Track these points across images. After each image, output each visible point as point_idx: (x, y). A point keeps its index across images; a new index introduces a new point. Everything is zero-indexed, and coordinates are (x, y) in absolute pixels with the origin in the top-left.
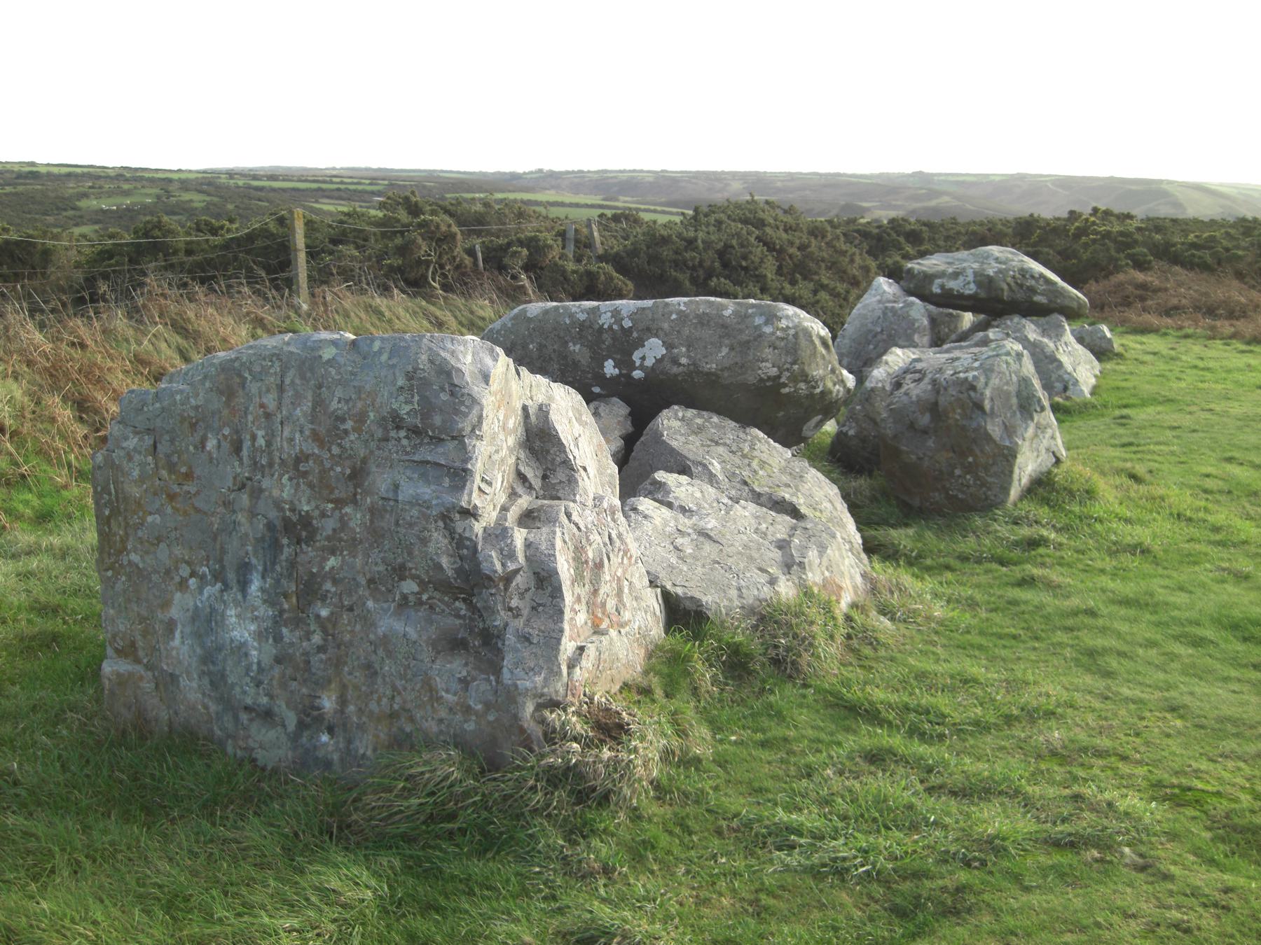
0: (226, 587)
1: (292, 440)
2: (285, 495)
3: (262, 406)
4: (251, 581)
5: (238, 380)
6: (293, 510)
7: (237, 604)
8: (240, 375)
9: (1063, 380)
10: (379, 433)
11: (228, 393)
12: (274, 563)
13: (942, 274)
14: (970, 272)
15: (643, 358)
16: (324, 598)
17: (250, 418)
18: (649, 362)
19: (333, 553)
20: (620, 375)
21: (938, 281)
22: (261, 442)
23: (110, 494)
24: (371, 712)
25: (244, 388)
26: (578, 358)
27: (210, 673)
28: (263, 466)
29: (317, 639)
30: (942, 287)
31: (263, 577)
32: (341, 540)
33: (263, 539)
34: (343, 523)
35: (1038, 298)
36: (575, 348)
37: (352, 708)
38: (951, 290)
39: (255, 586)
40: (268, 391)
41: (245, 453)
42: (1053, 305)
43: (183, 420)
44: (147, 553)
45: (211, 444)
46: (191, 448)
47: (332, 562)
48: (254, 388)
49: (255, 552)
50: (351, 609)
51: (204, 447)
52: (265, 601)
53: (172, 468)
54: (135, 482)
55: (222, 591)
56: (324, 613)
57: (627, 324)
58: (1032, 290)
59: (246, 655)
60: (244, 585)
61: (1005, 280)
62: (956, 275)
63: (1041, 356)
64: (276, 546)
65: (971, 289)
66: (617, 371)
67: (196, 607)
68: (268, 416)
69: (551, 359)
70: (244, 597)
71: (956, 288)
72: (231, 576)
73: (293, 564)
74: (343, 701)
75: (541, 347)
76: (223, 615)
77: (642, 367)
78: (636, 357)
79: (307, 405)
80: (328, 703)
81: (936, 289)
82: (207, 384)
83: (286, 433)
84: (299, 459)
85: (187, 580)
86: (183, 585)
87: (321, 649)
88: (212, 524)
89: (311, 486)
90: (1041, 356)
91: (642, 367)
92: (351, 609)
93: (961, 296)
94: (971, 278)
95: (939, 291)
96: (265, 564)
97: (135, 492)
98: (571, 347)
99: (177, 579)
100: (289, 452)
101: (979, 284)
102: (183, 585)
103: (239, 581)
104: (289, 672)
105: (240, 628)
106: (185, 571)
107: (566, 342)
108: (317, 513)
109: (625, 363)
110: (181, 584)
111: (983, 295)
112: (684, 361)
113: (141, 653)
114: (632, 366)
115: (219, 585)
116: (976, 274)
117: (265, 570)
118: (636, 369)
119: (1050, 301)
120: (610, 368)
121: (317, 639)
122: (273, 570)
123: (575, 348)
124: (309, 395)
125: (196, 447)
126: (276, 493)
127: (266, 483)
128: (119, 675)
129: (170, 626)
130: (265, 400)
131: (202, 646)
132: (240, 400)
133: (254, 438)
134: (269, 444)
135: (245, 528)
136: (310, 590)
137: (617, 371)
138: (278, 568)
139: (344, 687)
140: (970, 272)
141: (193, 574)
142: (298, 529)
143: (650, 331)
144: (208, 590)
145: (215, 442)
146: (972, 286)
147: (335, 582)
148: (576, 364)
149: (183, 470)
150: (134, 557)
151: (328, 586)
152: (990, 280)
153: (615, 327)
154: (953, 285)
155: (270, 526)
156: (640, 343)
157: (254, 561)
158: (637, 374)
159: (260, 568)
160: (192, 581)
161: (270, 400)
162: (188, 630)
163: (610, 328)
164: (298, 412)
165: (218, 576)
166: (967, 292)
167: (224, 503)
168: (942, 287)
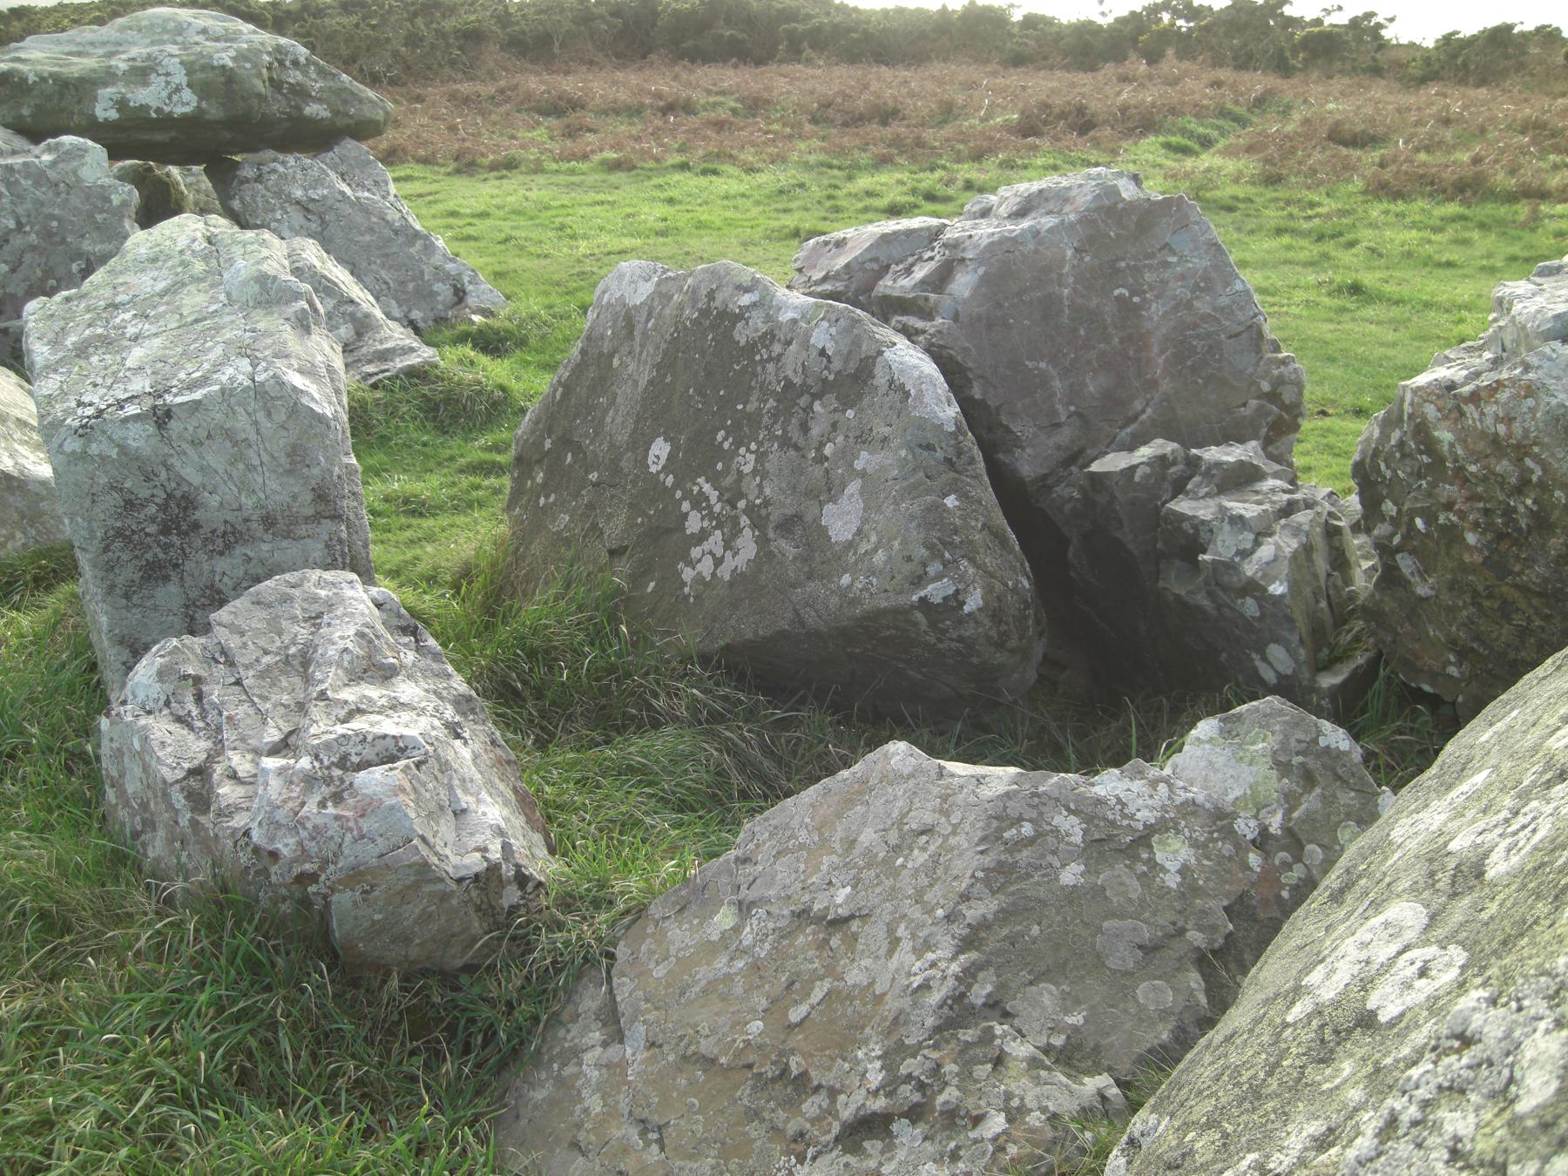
9: (448, 275)
13: (109, 77)
14: (173, 65)
21: (106, 93)
30: (122, 104)
35: (314, 110)
38: (144, 108)
42: (341, 122)
58: (300, 92)
61: (260, 75)
62: (142, 73)
63: (387, 232)
65: (186, 104)
71: (154, 104)
81: (104, 111)
90: (387, 232)
93: (165, 121)
94: (180, 77)
95: (113, 115)
111: (214, 112)
119: (336, 113)
140: (173, 65)
146: (187, 94)
152: (228, 76)
154: (148, 96)
166: (179, 110)
168: (122, 104)
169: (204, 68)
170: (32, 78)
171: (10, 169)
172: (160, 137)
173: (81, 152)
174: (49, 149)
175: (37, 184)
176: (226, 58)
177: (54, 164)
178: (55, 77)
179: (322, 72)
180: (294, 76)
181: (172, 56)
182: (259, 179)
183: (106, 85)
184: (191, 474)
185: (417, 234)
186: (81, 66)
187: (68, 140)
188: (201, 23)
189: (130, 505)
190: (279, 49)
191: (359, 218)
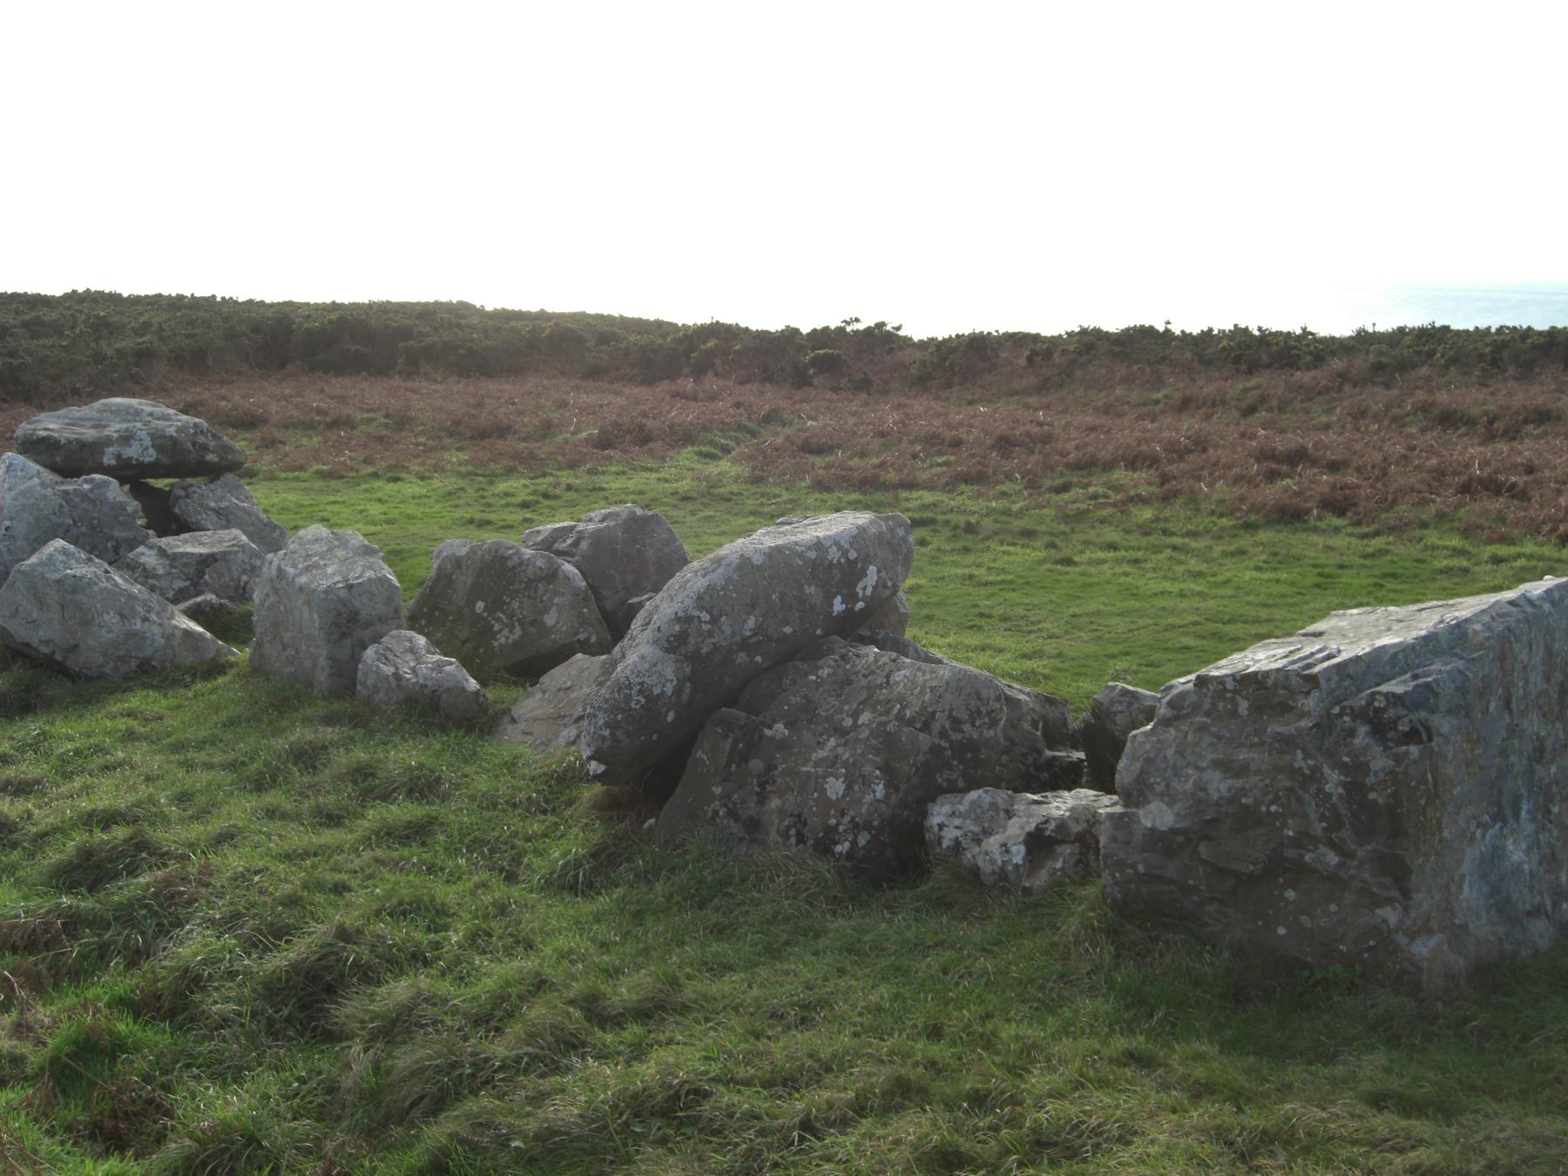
7: (1513, 831)
13: (108, 441)
14: (143, 435)
15: (864, 589)
18: (869, 592)
21: (111, 450)
23: (1426, 783)
30: (118, 457)
35: (211, 457)
36: (811, 590)
38: (130, 459)
41: (1514, 706)
57: (853, 555)
58: (205, 448)
62: (126, 439)
72: (1508, 811)
75: (782, 595)
76: (1504, 849)
78: (859, 589)
94: (148, 442)
95: (113, 462)
101: (160, 449)
102: (1472, 840)
105: (1516, 853)
114: (855, 599)
115: (1498, 825)
116: (153, 436)
119: (221, 458)
123: (811, 590)
140: (143, 435)
143: (867, 559)
144: (1490, 833)
146: (151, 451)
152: (174, 442)
154: (132, 452)
156: (863, 574)
158: (860, 605)
165: (1494, 820)
166: (147, 460)
168: (118, 457)
170: (63, 441)
171: (67, 492)
173: (107, 484)
174: (86, 481)
175: (83, 500)
176: (172, 431)
177: (91, 490)
179: (215, 437)
180: (201, 439)
182: (187, 496)
183: (108, 446)
184: (358, 605)
185: (276, 527)
186: (89, 434)
188: (150, 409)
189: (339, 614)
190: (196, 425)
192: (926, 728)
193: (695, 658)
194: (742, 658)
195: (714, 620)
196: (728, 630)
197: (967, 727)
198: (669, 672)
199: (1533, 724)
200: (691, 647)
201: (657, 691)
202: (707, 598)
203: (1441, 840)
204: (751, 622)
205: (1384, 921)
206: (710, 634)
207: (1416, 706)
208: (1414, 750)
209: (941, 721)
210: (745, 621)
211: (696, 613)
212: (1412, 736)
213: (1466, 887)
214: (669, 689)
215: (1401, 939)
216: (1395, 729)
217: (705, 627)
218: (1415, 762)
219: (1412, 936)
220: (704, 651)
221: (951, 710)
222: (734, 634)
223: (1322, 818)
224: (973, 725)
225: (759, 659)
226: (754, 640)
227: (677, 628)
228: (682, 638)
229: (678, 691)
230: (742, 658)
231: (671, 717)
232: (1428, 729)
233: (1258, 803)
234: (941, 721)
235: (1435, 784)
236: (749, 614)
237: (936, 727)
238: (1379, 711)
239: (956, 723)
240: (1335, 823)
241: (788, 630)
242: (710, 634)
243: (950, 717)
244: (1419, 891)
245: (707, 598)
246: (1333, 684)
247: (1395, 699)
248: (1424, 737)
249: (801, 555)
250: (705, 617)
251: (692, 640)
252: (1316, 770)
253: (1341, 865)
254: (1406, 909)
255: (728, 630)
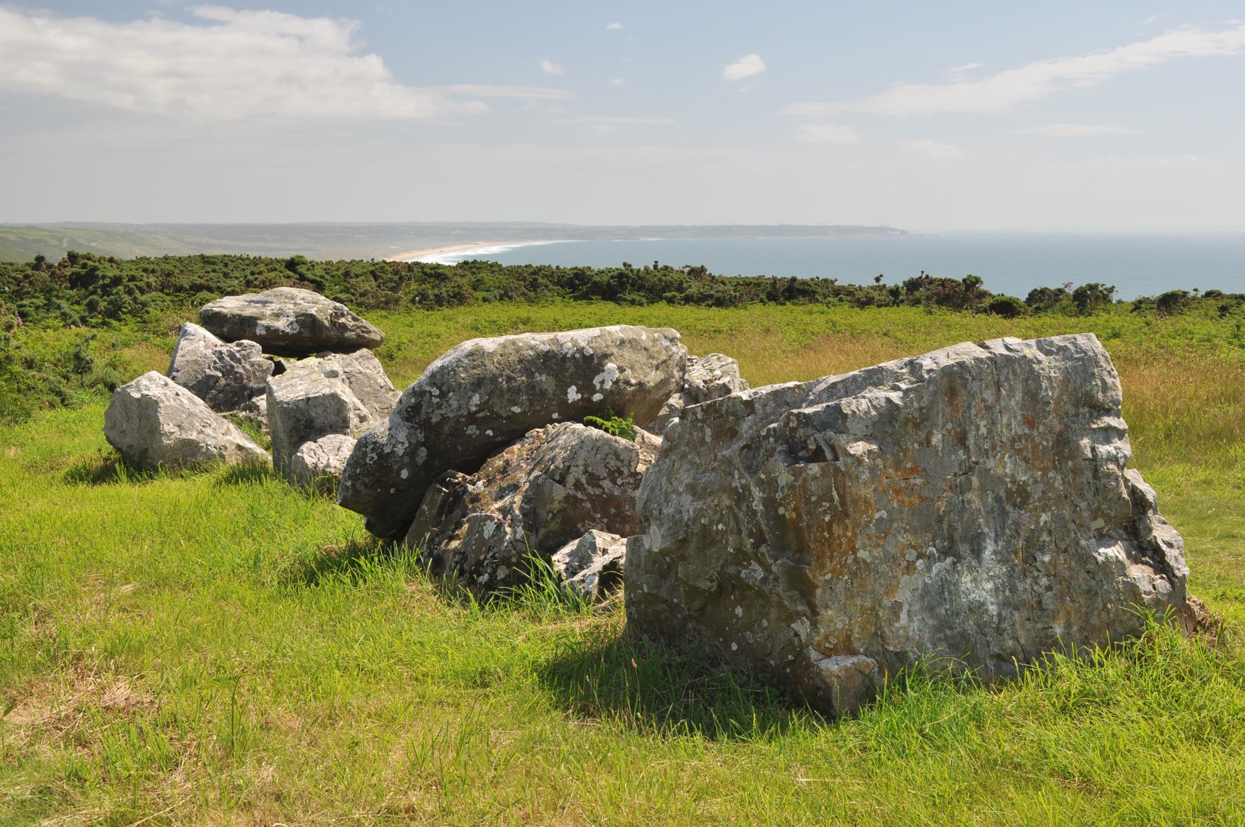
0: (959, 558)
1: (1009, 425)
2: (1007, 470)
3: (983, 400)
4: (985, 548)
5: (959, 381)
6: (1013, 482)
7: (971, 569)
8: (962, 377)
10: (1072, 411)
11: (952, 393)
12: (1003, 529)
15: (602, 382)
16: (1042, 549)
17: (973, 412)
18: (608, 385)
19: (1044, 511)
20: (582, 399)
22: (983, 430)
23: (832, 500)
24: (1094, 626)
25: (965, 387)
26: (545, 387)
27: (946, 638)
28: (986, 451)
29: (1044, 581)
31: (996, 542)
32: (1050, 498)
33: (992, 511)
34: (1049, 486)
35: (348, 334)
37: (1075, 628)
39: (987, 554)
40: (987, 387)
41: (971, 442)
43: (907, 420)
44: (878, 545)
45: (936, 439)
46: (916, 445)
47: (1044, 518)
48: (975, 386)
49: (987, 522)
50: (1066, 551)
51: (928, 442)
52: (999, 562)
53: (898, 465)
54: (865, 484)
55: (954, 563)
56: (1047, 559)
58: (344, 327)
59: (987, 610)
60: (977, 552)
64: (1004, 514)
66: (579, 396)
67: (925, 584)
68: (988, 408)
69: (519, 390)
70: (980, 562)
71: (282, 328)
72: (964, 548)
73: (1016, 523)
74: (1068, 625)
76: (956, 584)
77: (602, 391)
78: (596, 381)
79: (1019, 396)
80: (1058, 630)
81: (260, 331)
82: (931, 388)
83: (1005, 421)
84: (1013, 441)
85: (914, 563)
86: (910, 568)
87: (1049, 588)
88: (939, 509)
89: (1026, 460)
91: (602, 391)
92: (1066, 551)
95: (264, 332)
96: (996, 531)
97: (866, 492)
98: (538, 377)
99: (904, 564)
100: (1006, 435)
102: (910, 568)
103: (973, 551)
104: (1025, 614)
106: (911, 555)
107: (533, 373)
108: (1031, 481)
109: (587, 388)
110: (907, 568)
112: (633, 381)
113: (856, 645)
115: (949, 560)
117: (997, 535)
118: (596, 392)
120: (573, 395)
121: (1044, 581)
122: (1004, 533)
124: (1019, 387)
125: (921, 444)
126: (1000, 471)
127: (991, 463)
128: (847, 669)
129: (896, 608)
130: (985, 396)
131: (937, 617)
132: (962, 397)
133: (978, 428)
134: (990, 431)
135: (977, 504)
136: (1033, 547)
137: (579, 396)
138: (1007, 531)
139: (1068, 613)
141: (920, 556)
142: (1020, 497)
145: (940, 436)
147: (1050, 533)
148: (543, 393)
149: (909, 465)
150: (862, 554)
151: (1045, 537)
153: (577, 356)
154: (281, 324)
155: (998, 499)
157: (986, 530)
158: (597, 397)
159: (993, 535)
160: (920, 564)
161: (989, 395)
162: (916, 607)
163: (573, 356)
164: (1013, 402)
165: (945, 553)
167: (951, 487)
168: (268, 328)
169: (303, 315)
172: (282, 343)
174: (238, 345)
178: (240, 316)
181: (290, 308)
184: (314, 415)
187: (245, 342)
188: (301, 295)
189: (298, 420)
191: (366, 381)
192: (562, 481)
193: (426, 426)
194: (472, 430)
195: (443, 395)
196: (455, 404)
197: (606, 484)
198: (402, 436)
199: (1006, 466)
200: (423, 416)
201: (387, 450)
202: (438, 376)
203: (856, 560)
204: (476, 399)
205: (796, 634)
206: (439, 406)
207: (824, 426)
208: (815, 468)
209: (576, 473)
210: (470, 398)
211: (428, 388)
212: (817, 456)
213: (904, 616)
214: (400, 450)
215: (814, 655)
216: (805, 448)
217: (435, 400)
218: (815, 478)
219: (827, 654)
220: (434, 420)
221: (586, 466)
222: (460, 408)
223: (750, 535)
224: (614, 482)
225: (490, 432)
226: (481, 415)
227: (413, 400)
228: (416, 408)
229: (412, 452)
230: (472, 430)
231: (404, 474)
232: (833, 448)
233: (711, 522)
234: (576, 473)
235: (843, 502)
236: (474, 391)
237: (571, 480)
238: (793, 430)
239: (594, 479)
240: (760, 540)
241: (517, 409)
242: (439, 406)
243: (585, 472)
244: (827, 607)
245: (438, 376)
246: (768, 409)
247: (806, 420)
248: (829, 456)
249: (532, 348)
250: (436, 392)
251: (423, 411)
252: (746, 488)
253: (764, 580)
254: (814, 624)
255: (455, 404)
